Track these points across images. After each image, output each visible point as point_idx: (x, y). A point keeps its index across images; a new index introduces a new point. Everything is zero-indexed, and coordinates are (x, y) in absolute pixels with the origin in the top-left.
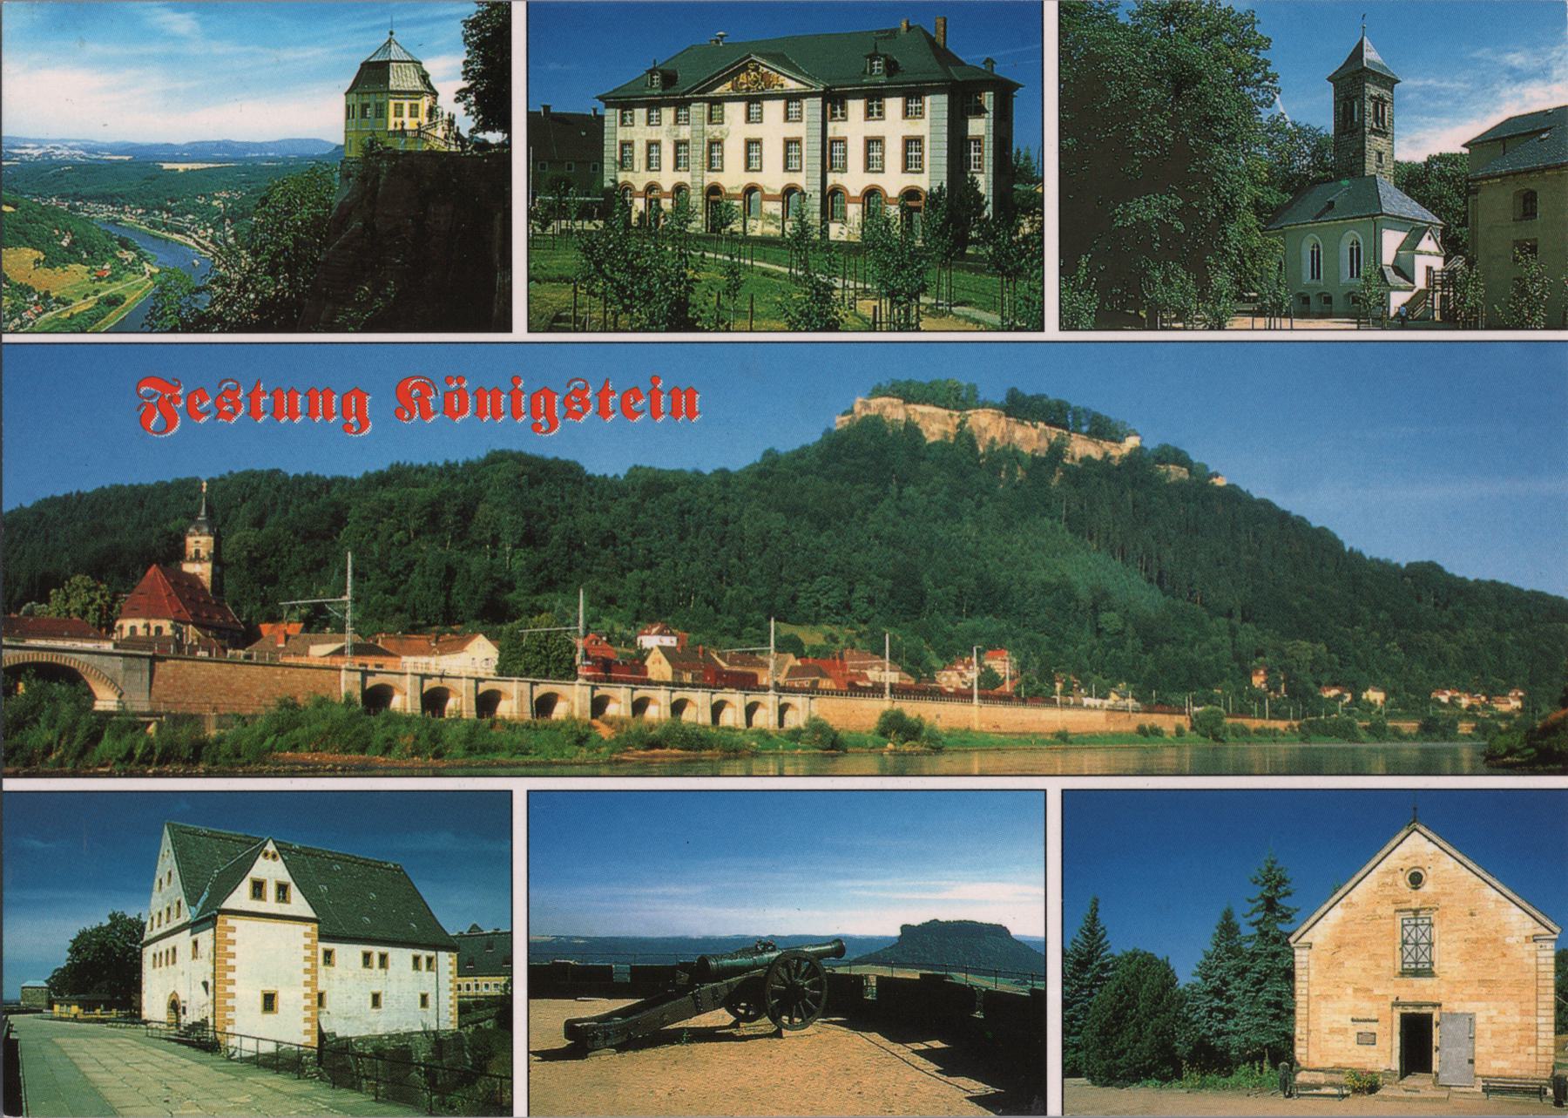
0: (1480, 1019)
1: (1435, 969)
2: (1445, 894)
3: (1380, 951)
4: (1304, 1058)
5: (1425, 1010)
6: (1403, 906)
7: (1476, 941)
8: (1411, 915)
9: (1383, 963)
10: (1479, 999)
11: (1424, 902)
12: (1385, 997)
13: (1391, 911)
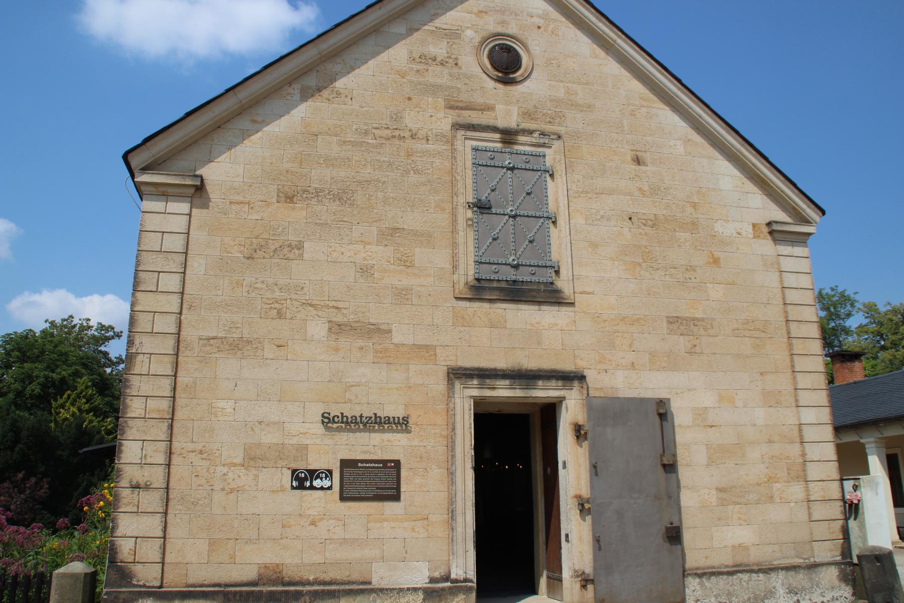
0: (681, 415)
1: (563, 283)
2: (575, 105)
3: (412, 220)
4: (150, 551)
5: (544, 392)
6: (474, 118)
7: (655, 223)
8: (493, 142)
9: (421, 255)
10: (671, 363)
11: (527, 114)
12: (425, 351)
13: (444, 122)
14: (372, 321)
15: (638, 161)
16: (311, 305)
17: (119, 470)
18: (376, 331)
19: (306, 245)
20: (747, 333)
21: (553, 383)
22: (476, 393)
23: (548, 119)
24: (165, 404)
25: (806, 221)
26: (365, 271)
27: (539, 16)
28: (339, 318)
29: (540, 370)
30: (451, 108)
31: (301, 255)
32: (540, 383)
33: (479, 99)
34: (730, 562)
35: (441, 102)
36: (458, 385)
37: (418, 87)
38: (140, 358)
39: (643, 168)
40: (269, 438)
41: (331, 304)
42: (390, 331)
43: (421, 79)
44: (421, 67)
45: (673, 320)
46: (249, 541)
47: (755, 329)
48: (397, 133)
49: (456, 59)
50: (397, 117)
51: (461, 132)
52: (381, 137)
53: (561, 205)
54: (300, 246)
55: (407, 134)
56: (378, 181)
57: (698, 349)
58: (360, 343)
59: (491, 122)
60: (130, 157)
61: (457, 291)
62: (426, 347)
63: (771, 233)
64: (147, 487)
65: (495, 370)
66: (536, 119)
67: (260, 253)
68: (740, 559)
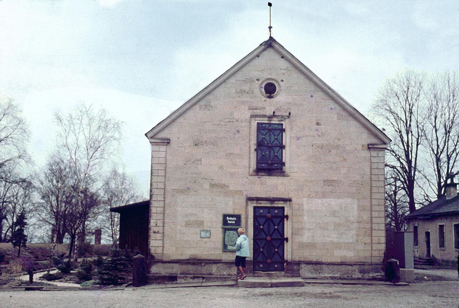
13: (248, 114)
14: (223, 183)
15: (318, 124)
16: (205, 179)
17: (150, 228)
18: (224, 186)
19: (203, 160)
20: (355, 185)
21: (281, 202)
22: (255, 205)
23: (285, 111)
24: (162, 209)
25: (385, 143)
26: (221, 167)
27: (284, 69)
28: (213, 183)
29: (276, 198)
30: (250, 109)
31: (201, 163)
32: (276, 202)
33: (260, 105)
34: (339, 261)
35: (247, 107)
36: (249, 202)
37: (239, 102)
38: (154, 195)
39: (320, 126)
40: (193, 218)
41: (211, 178)
42: (229, 186)
43: (240, 100)
44: (240, 95)
45: (325, 181)
46: (187, 248)
47: (358, 184)
48: (231, 120)
49: (253, 90)
50: (232, 114)
51: (253, 119)
52: (226, 122)
53: (287, 142)
54: (200, 160)
55: (235, 120)
56: (225, 137)
57: (334, 191)
58: (220, 190)
59: (264, 114)
60: (147, 134)
61: (250, 173)
62: (240, 191)
63: (369, 148)
64: (158, 232)
65: (262, 198)
66: (281, 111)
67: (189, 163)
68: (343, 260)
